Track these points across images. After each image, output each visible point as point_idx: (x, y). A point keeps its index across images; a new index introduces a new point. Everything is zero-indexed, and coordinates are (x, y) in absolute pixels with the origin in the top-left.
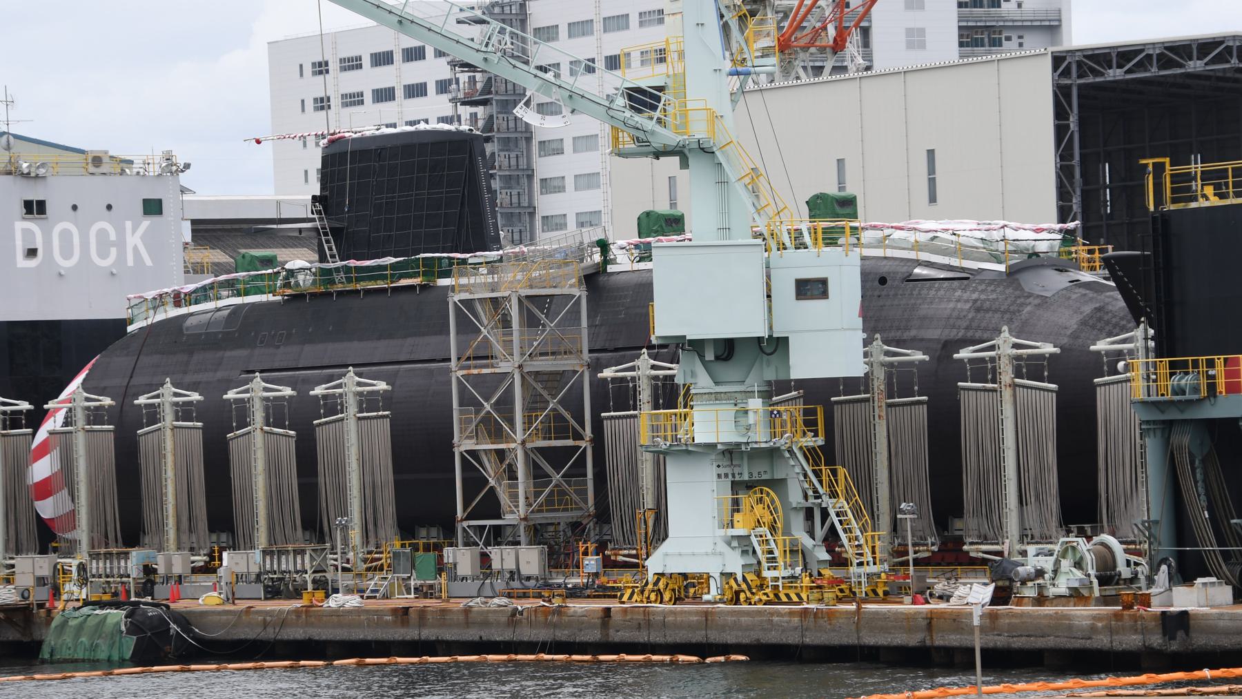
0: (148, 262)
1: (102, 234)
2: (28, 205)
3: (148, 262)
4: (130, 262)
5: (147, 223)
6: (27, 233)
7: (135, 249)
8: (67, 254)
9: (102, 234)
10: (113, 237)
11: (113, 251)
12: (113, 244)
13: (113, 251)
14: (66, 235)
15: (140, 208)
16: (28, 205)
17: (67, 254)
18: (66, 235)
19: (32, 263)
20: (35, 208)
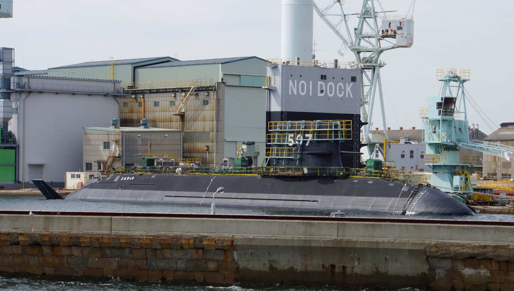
0: (352, 97)
1: (340, 86)
2: (322, 76)
3: (352, 97)
4: (347, 96)
5: (352, 84)
6: (321, 85)
8: (331, 93)
9: (340, 86)
10: (343, 88)
11: (343, 92)
12: (343, 90)
13: (343, 92)
14: (331, 86)
16: (322, 76)
17: (331, 93)
18: (331, 86)
20: (323, 77)
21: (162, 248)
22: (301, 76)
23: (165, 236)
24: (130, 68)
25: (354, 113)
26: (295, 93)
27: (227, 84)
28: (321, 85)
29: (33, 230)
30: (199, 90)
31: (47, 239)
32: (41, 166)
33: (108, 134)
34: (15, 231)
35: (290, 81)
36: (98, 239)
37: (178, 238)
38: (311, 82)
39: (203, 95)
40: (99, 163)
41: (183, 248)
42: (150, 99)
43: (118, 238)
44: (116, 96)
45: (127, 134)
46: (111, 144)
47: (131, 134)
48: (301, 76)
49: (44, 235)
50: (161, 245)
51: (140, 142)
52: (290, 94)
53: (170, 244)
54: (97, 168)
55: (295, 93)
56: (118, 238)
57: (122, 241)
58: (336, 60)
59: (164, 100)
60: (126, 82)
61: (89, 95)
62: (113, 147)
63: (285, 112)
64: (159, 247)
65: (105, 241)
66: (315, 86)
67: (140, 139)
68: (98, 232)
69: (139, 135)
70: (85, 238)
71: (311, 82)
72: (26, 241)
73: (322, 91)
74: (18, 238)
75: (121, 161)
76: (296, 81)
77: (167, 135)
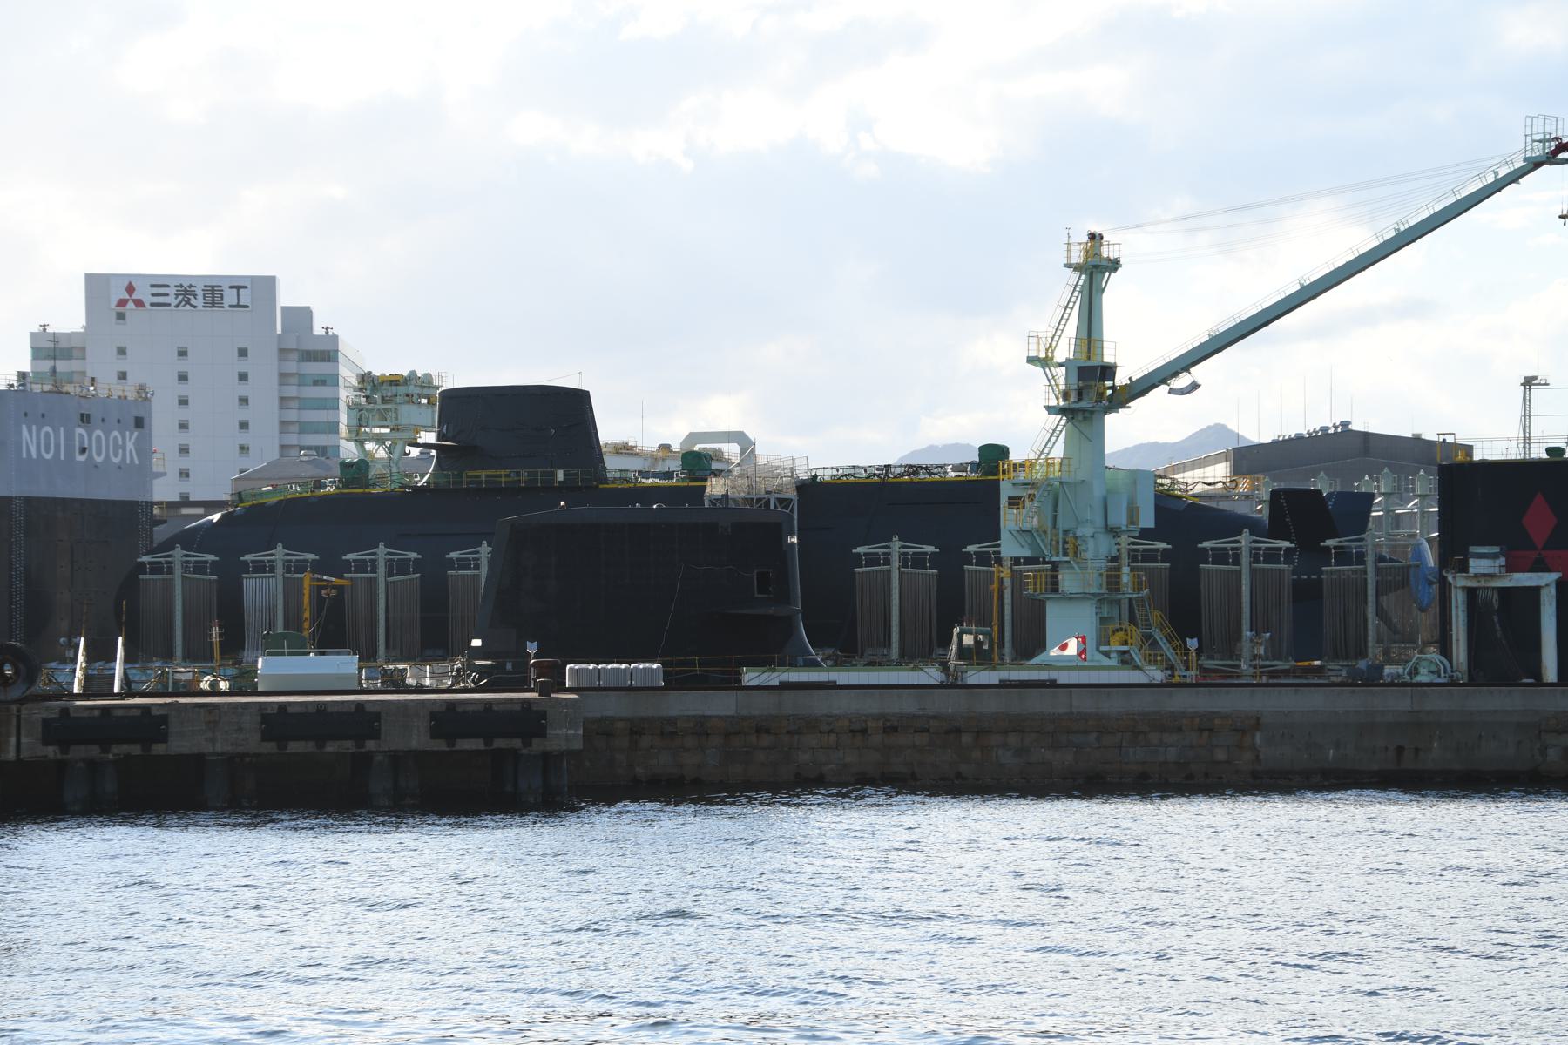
8: (99, 454)
15: (132, 422)
17: (99, 454)
20: (85, 419)
25: (14, 491)
28: (81, 436)
66: (69, 437)
73: (83, 450)
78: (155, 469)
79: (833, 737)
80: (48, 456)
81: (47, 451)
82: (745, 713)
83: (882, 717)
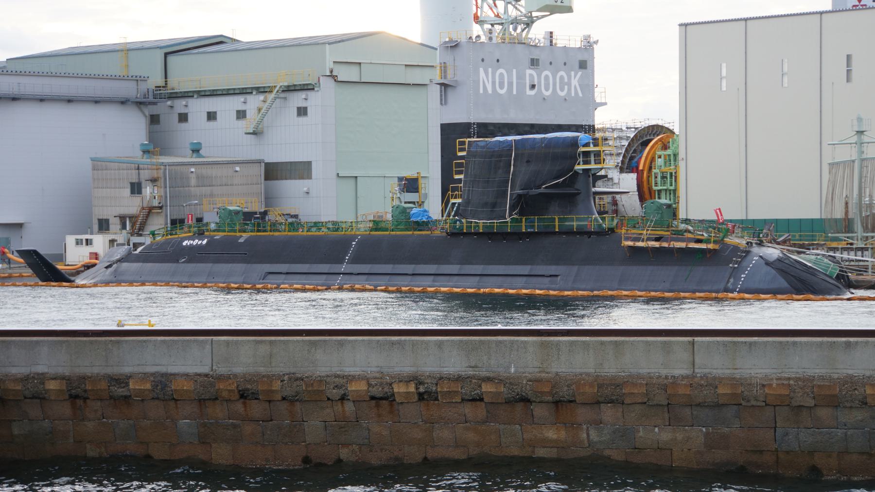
0: (581, 95)
1: (562, 78)
2: (532, 60)
3: (581, 95)
4: (573, 95)
5: (580, 73)
6: (531, 75)
7: (575, 87)
8: (547, 89)
9: (562, 78)
10: (566, 80)
11: (566, 87)
13: (566, 87)
14: (547, 77)
15: (577, 65)
16: (532, 60)
17: (547, 89)
18: (547, 77)
19: (533, 92)
20: (534, 63)
21: (815, 405)
22: (498, 61)
23: (822, 378)
24: (159, 56)
26: (490, 90)
27: (339, 79)
28: (531, 75)
29: (513, 370)
30: (290, 89)
31: (547, 390)
32: (20, 226)
33: (138, 169)
34: (471, 372)
35: (481, 70)
36: (665, 388)
37: (851, 382)
38: (514, 71)
39: (297, 99)
40: (123, 218)
41: (866, 404)
42: (198, 108)
43: (711, 385)
44: (141, 103)
45: (173, 167)
46: (143, 185)
47: (179, 167)
48: (498, 61)
49: (538, 381)
50: (814, 398)
51: (193, 182)
52: (481, 91)
53: (835, 396)
54: (119, 227)
55: (490, 90)
56: (713, 383)
57: (721, 391)
58: (551, 33)
59: (226, 107)
60: (157, 79)
61: (96, 102)
62: (147, 190)
63: (474, 124)
64: (811, 403)
65: (681, 391)
66: (521, 77)
67: (193, 175)
68: (664, 372)
69: (193, 170)
70: (635, 385)
71: (514, 71)
72: (499, 394)
73: (533, 87)
74: (480, 386)
75: (163, 214)
76: (490, 70)
77: (238, 169)
78: (598, 100)
79: (349, 407)
80: (502, 92)
81: (547, 90)
82: (222, 370)
83: (417, 380)
